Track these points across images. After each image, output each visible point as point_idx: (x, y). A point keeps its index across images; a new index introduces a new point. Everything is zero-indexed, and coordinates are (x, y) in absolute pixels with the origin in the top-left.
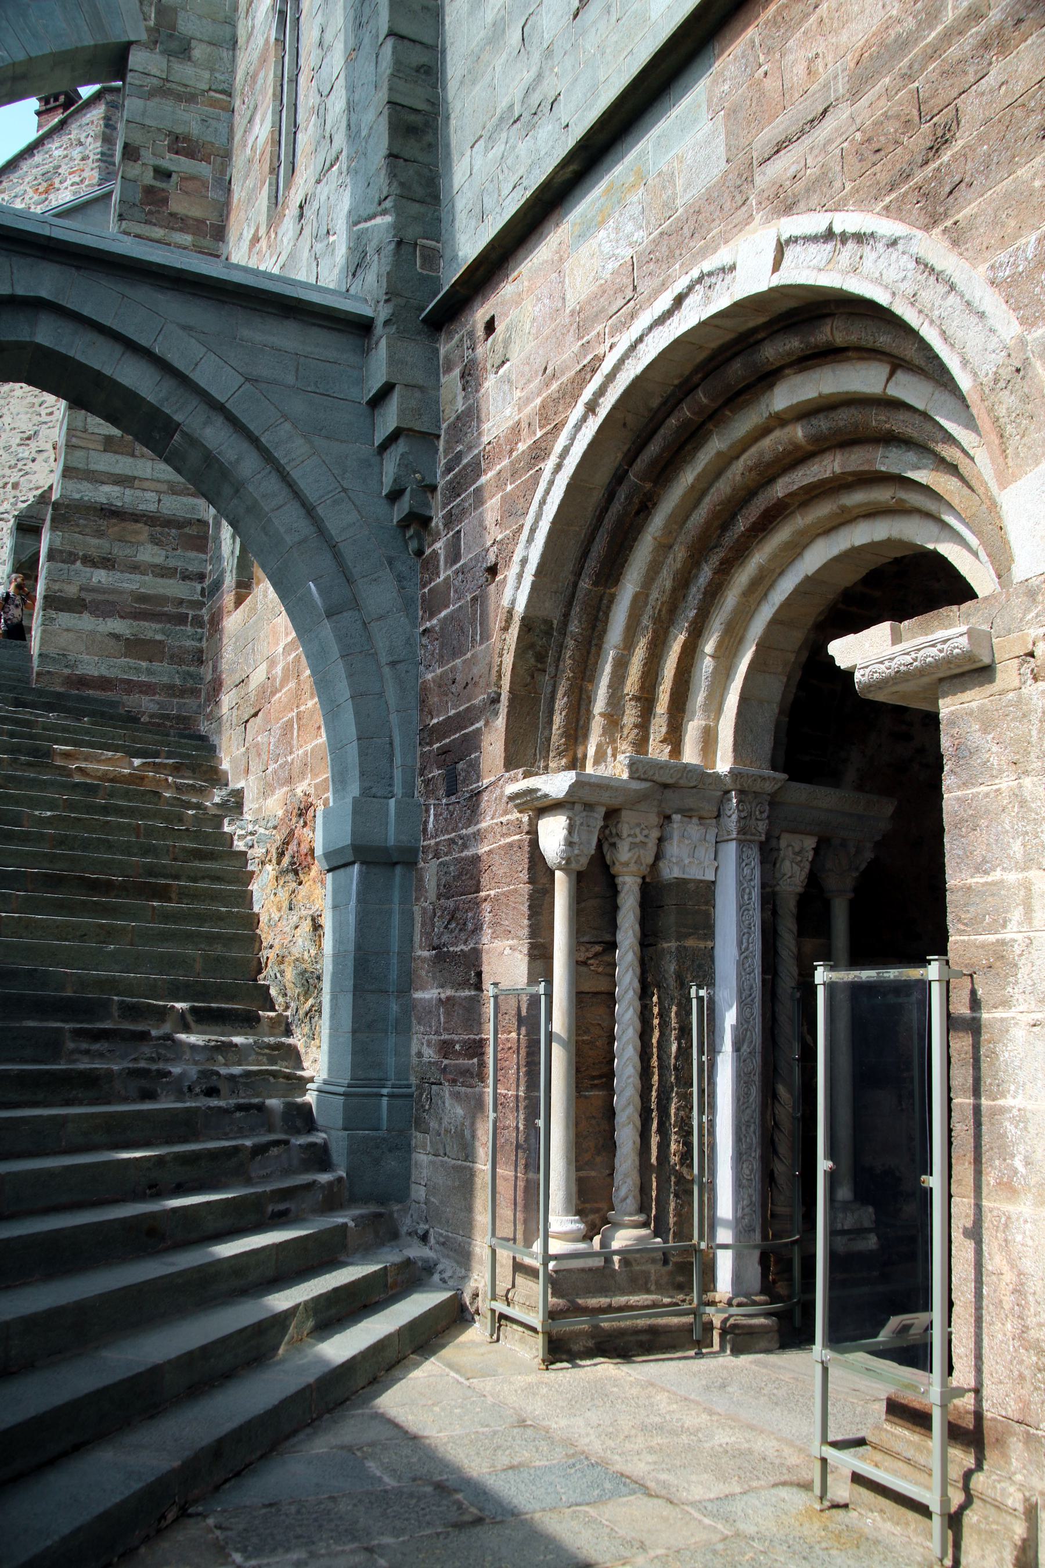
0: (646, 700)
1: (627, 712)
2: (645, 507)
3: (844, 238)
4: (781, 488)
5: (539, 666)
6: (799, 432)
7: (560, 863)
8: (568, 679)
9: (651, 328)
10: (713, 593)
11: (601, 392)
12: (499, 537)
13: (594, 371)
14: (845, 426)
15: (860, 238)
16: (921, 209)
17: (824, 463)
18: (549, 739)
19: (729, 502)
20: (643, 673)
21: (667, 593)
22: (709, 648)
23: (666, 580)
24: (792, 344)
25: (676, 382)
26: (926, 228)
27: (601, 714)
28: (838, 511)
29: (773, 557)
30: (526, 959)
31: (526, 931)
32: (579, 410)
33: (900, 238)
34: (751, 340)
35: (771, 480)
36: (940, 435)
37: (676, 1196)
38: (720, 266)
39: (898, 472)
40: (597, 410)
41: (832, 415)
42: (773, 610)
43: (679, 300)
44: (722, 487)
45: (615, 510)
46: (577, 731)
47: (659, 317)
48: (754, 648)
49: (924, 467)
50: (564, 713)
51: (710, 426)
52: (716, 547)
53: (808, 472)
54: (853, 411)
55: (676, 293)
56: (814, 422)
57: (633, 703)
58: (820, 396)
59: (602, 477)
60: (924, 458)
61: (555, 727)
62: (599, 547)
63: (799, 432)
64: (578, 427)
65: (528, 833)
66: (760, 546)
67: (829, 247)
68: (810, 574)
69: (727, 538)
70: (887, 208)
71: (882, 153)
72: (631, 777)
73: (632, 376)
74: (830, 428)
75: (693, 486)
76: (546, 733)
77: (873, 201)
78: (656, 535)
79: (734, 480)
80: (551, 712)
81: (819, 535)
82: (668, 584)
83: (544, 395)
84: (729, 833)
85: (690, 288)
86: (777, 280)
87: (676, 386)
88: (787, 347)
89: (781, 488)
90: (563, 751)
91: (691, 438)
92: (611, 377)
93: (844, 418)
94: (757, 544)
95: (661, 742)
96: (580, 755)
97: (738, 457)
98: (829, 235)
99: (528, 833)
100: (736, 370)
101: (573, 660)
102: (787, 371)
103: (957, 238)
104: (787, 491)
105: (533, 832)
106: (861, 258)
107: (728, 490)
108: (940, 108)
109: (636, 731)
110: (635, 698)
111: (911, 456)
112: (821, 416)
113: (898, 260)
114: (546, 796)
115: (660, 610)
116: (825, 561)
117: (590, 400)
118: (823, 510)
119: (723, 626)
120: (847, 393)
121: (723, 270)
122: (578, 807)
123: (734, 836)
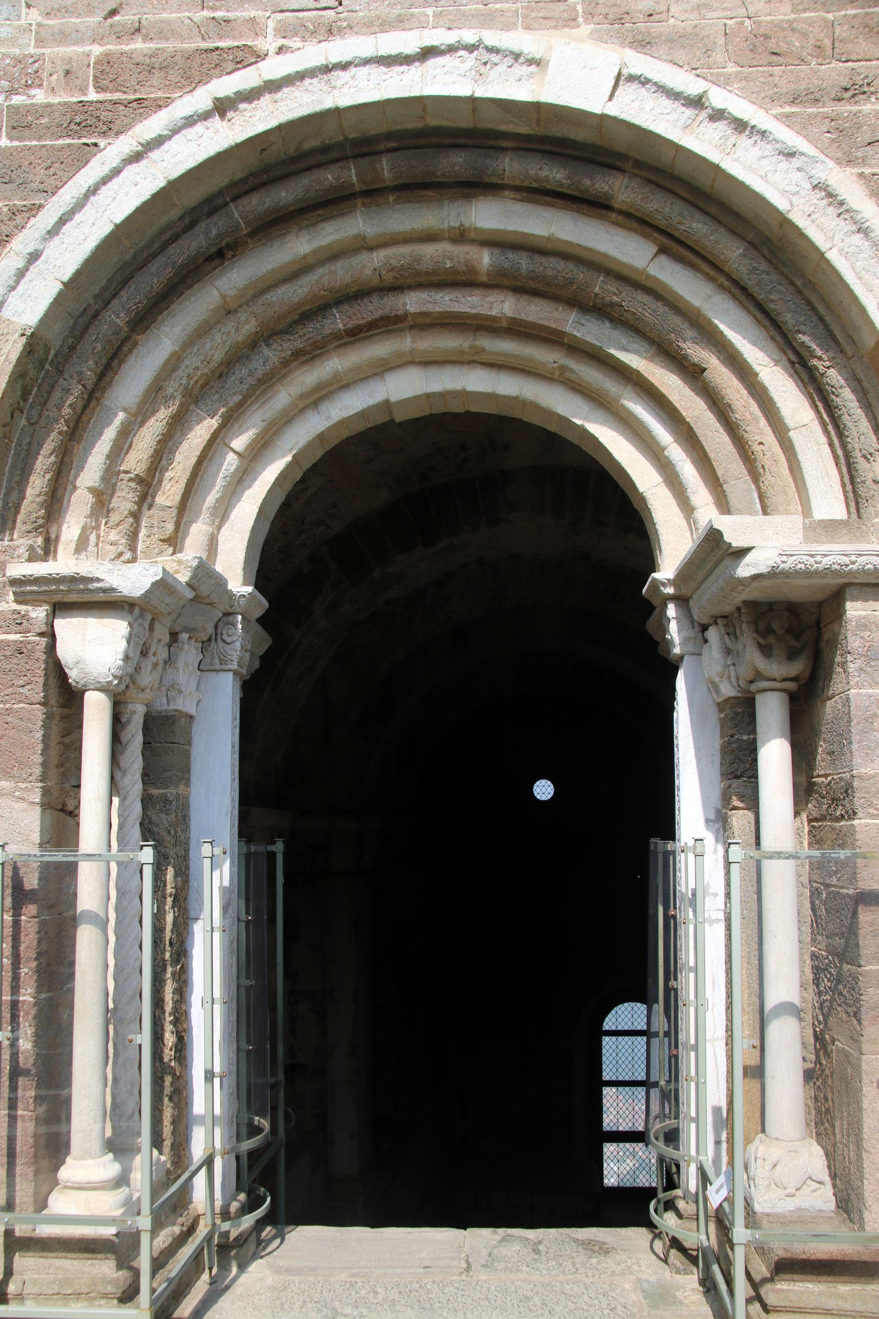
0: (147, 486)
1: (119, 493)
2: (220, 255)
3: (718, 115)
5: (22, 403)
6: (485, 259)
7: (110, 683)
8: (60, 433)
9: (367, 62)
10: (266, 383)
11: (250, 96)
13: (240, 64)
14: (555, 277)
15: (740, 126)
16: (833, 141)
17: (491, 299)
18: (18, 507)
19: (338, 291)
20: (155, 450)
21: (213, 365)
22: (240, 443)
23: (216, 348)
24: (555, 174)
25: (353, 135)
27: (91, 490)
28: (467, 350)
29: (358, 368)
30: (38, 809)
31: (37, 771)
32: (201, 98)
33: (802, 154)
34: (490, 143)
35: (396, 289)
36: (690, 333)
37: (171, 1099)
38: (516, 48)
39: (598, 344)
40: (230, 114)
41: (543, 259)
42: (328, 424)
43: (427, 53)
44: (340, 273)
45: (194, 245)
46: (54, 504)
47: (389, 57)
48: (289, 458)
49: (636, 352)
50: (48, 476)
51: (359, 202)
52: (287, 333)
53: (462, 300)
54: (571, 266)
55: (428, 43)
56: (512, 255)
57: (133, 485)
58: (549, 239)
59: (193, 197)
60: (635, 342)
61: (30, 492)
62: (154, 278)
64: (190, 121)
65: (41, 634)
66: (342, 351)
67: (689, 112)
68: (393, 399)
69: (307, 327)
70: (788, 116)
72: (189, 585)
73: (328, 103)
74: (531, 271)
75: (304, 257)
76: (14, 496)
77: (767, 100)
80: (24, 471)
81: (412, 363)
82: (218, 356)
83: (110, 47)
84: (222, 662)
85: (451, 49)
86: (612, 110)
87: (346, 139)
89: (413, 302)
90: (40, 527)
92: (272, 86)
93: (553, 267)
94: (338, 347)
95: (161, 540)
96: (53, 536)
97: (371, 249)
98: (697, 102)
99: (41, 634)
100: (455, 163)
101: (74, 409)
102: (507, 193)
104: (424, 309)
105: (51, 635)
106: (734, 145)
107: (348, 279)
109: (131, 520)
110: (139, 480)
111: (618, 335)
112: (524, 255)
113: (787, 172)
114: (113, 590)
115: (196, 382)
116: (419, 392)
117: (228, 98)
118: (449, 342)
119: (264, 424)
120: (591, 250)
121: (517, 56)
122: (137, 611)
123: (235, 666)
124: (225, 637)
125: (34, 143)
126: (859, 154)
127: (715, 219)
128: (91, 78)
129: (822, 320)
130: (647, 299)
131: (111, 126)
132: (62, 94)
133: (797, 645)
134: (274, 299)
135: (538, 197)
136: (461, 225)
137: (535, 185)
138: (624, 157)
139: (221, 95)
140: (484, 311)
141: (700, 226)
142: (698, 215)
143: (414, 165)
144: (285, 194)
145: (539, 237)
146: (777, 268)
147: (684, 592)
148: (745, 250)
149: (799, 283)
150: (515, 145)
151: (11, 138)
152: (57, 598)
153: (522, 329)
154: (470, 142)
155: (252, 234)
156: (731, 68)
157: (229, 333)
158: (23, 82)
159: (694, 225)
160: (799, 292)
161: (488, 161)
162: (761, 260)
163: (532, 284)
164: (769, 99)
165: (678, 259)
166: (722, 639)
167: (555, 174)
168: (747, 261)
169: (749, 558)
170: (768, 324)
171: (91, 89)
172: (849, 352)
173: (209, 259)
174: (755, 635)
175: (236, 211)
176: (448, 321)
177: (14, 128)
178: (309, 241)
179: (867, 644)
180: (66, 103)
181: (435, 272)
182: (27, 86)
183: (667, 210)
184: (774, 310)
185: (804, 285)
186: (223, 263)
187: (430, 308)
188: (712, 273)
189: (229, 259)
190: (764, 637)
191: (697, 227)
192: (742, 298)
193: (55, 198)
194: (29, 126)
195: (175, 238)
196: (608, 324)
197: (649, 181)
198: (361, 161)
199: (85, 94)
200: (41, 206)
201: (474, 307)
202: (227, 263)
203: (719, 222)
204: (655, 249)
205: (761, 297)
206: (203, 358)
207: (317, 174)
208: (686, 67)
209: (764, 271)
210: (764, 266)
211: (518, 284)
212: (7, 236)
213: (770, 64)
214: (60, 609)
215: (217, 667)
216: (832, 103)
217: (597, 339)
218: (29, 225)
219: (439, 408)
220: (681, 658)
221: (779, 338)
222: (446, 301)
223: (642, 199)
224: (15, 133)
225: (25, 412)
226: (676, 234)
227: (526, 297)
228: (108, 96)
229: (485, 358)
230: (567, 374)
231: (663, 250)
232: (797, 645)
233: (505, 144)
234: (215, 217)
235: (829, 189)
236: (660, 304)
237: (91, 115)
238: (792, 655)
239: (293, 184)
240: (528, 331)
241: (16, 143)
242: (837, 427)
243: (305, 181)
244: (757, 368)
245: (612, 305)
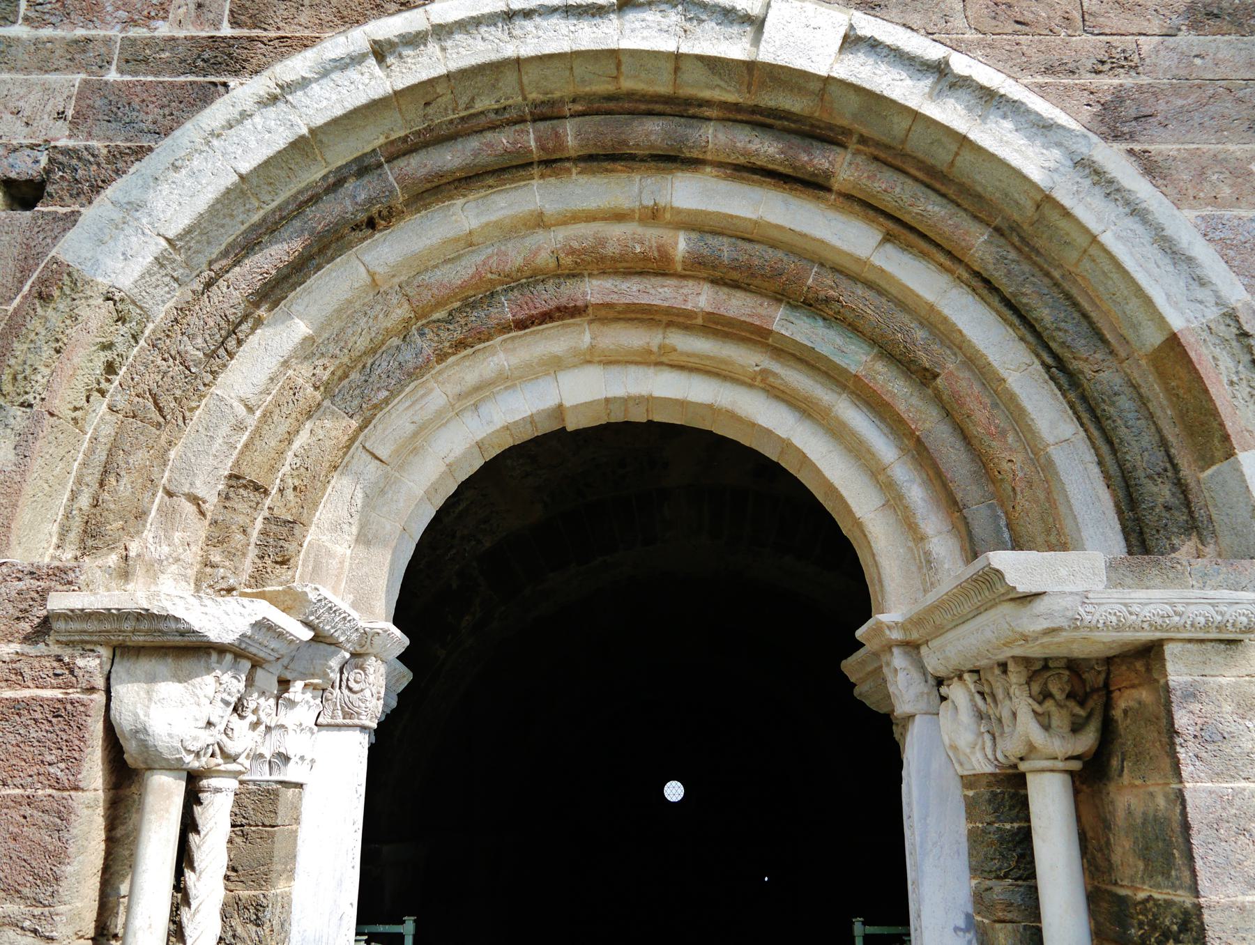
4: (594, 290)
11: (414, 40)
12: (63, 143)
17: (685, 291)
24: (767, 148)
26: (1105, 139)
28: (655, 349)
34: (691, 111)
35: (574, 275)
39: (810, 345)
41: (747, 246)
45: (338, 209)
47: (579, 6)
51: (535, 171)
53: (652, 291)
54: (780, 254)
56: (713, 241)
58: (756, 223)
63: (681, 245)
66: (510, 345)
69: (469, 315)
71: (1027, 29)
77: (1016, 69)
78: (379, 270)
79: (536, 254)
88: (753, 147)
89: (594, 290)
91: (510, 169)
93: (760, 255)
100: (652, 132)
102: (708, 169)
103: (1150, 167)
104: (608, 300)
108: (1114, 31)
124: (352, 684)
125: (150, 78)
126: (1126, 129)
127: (953, 201)
128: (227, 12)
129: (1085, 316)
130: (870, 294)
131: (247, 65)
132: (190, 27)
133: (1082, 713)
134: (432, 280)
135: (745, 175)
136: (655, 204)
137: (742, 160)
138: (847, 132)
139: (380, 36)
140: (679, 304)
141: (937, 209)
142: (934, 197)
143: (603, 131)
144: (450, 158)
145: (745, 219)
146: (1028, 258)
147: (915, 636)
148: (990, 236)
149: (1056, 274)
150: (721, 114)
151: (121, 72)
152: (115, 639)
153: (719, 327)
154: (668, 109)
155: (407, 204)
156: (971, 36)
157: (376, 317)
158: (145, 13)
159: (930, 208)
160: (1056, 285)
161: (689, 131)
162: (1009, 248)
163: (735, 275)
164: (1017, 65)
165: (907, 247)
166: (972, 700)
167: (767, 148)
168: (994, 249)
169: (1040, 606)
170: (1016, 321)
171: (226, 24)
172: (1123, 354)
173: (356, 227)
174: (1030, 701)
175: (390, 174)
176: (633, 316)
177: (127, 61)
178: (477, 215)
179: (1200, 721)
180: (193, 38)
181: (622, 258)
182: (149, 17)
183: (898, 190)
184: (1027, 304)
185: (1063, 276)
186: (372, 235)
187: (614, 298)
188: (948, 263)
189: (380, 231)
190: (1040, 703)
191: (931, 210)
192: (985, 292)
193: (168, 141)
194: (145, 61)
195: (315, 199)
196: (821, 323)
197: (876, 159)
198: (541, 125)
199: (218, 29)
200: (150, 149)
201: (666, 299)
202: (377, 235)
203: (959, 205)
204: (880, 237)
205: (1008, 290)
206: (342, 344)
207: (489, 136)
208: (923, 31)
209: (1013, 261)
210: (1013, 255)
211: (718, 274)
212: (103, 181)
213: (1015, 33)
214: (122, 655)
215: (340, 721)
216: (1089, 75)
217: (808, 339)
218: (132, 170)
219: (617, 417)
220: (911, 717)
221: (1029, 337)
222: (633, 291)
223: (869, 177)
224: (125, 67)
225: (108, 396)
226: (907, 218)
227: (726, 290)
228: (245, 32)
229: (674, 357)
230: (771, 379)
231: (888, 238)
232: (1082, 713)
233: (708, 112)
234: (365, 180)
235: (1096, 166)
236: (884, 300)
237: (224, 53)
238: (1076, 728)
239: (460, 147)
240: (726, 329)
241: (127, 78)
242: (1110, 442)
243: (474, 143)
244: (1003, 373)
245: (827, 300)
